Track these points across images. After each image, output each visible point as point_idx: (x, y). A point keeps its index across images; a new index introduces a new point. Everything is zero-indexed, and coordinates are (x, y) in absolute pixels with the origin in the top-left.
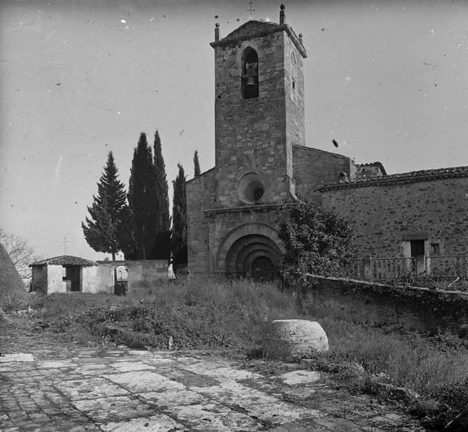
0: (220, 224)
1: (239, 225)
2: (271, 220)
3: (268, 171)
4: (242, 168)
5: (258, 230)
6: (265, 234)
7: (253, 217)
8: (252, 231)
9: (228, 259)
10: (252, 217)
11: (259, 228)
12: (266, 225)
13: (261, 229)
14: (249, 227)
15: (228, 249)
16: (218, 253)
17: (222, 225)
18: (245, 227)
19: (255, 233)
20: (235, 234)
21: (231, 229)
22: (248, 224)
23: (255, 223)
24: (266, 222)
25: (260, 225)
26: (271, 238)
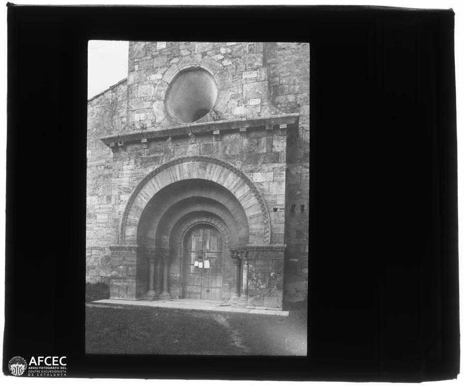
0: (132, 161)
1: (164, 162)
2: (227, 152)
3: (225, 63)
4: (175, 60)
5: (201, 171)
6: (215, 180)
7: (192, 148)
8: (189, 174)
9: (144, 225)
10: (190, 147)
11: (205, 169)
12: (217, 162)
13: (208, 170)
14: (185, 165)
15: (143, 206)
16: (126, 213)
17: (136, 162)
18: (177, 166)
19: (195, 176)
20: (160, 174)
21: (150, 170)
22: (182, 160)
23: (195, 158)
24: (219, 156)
25: (204, 160)
26: (225, 185)
